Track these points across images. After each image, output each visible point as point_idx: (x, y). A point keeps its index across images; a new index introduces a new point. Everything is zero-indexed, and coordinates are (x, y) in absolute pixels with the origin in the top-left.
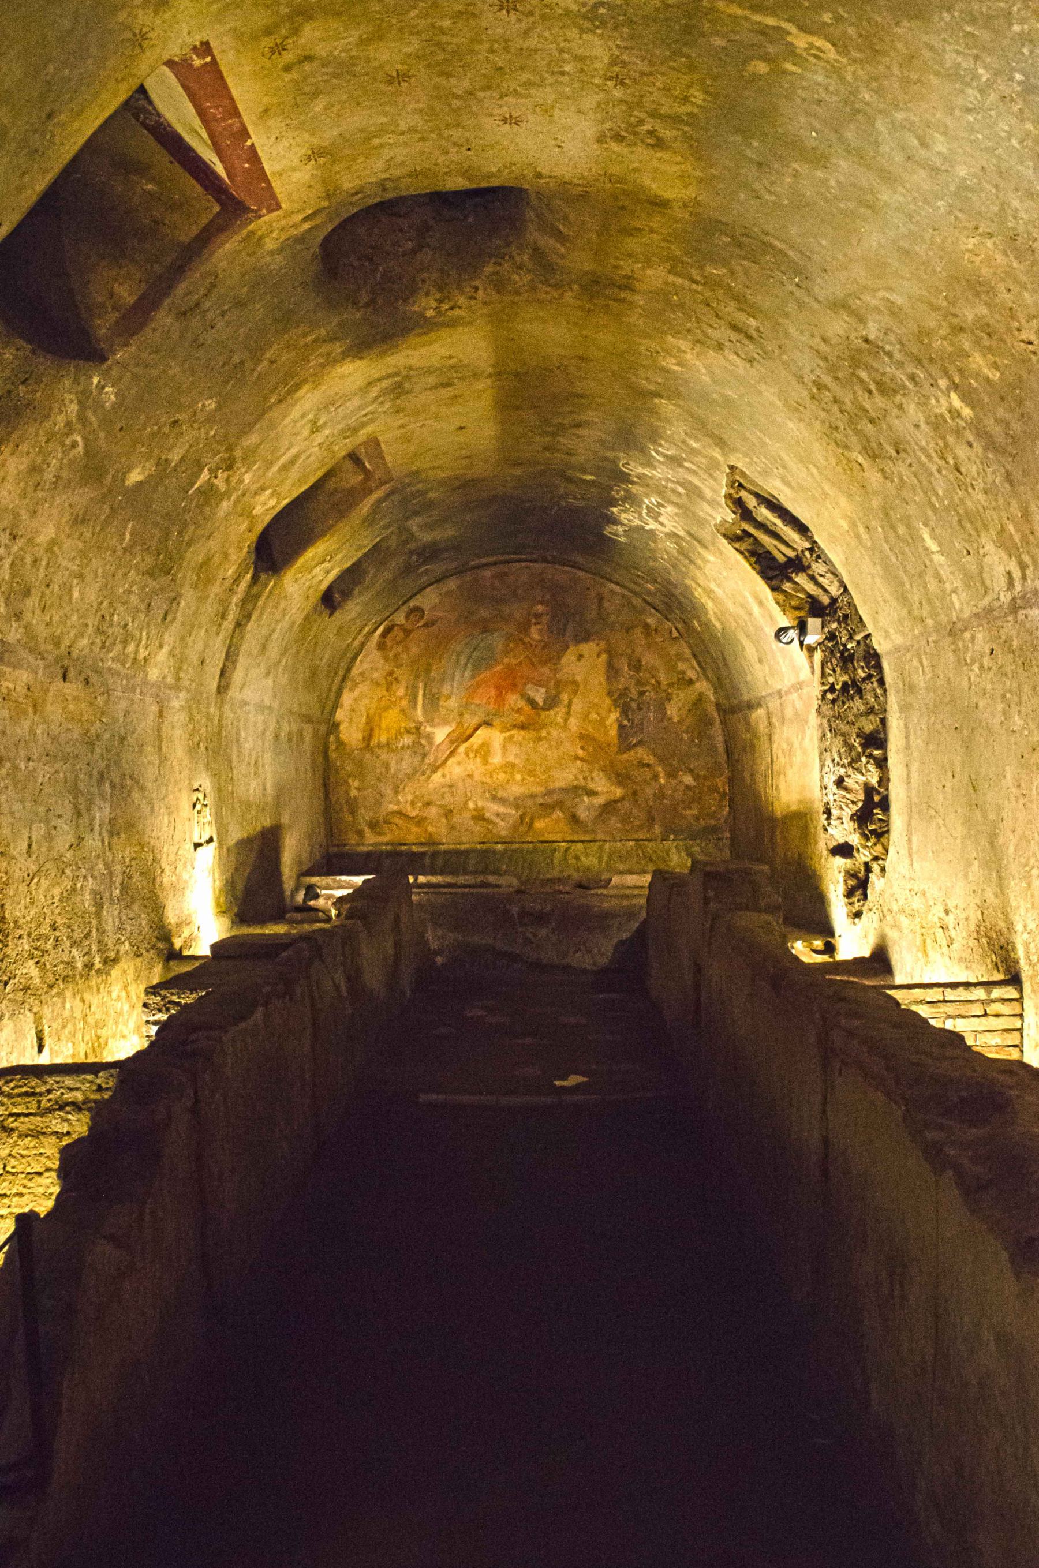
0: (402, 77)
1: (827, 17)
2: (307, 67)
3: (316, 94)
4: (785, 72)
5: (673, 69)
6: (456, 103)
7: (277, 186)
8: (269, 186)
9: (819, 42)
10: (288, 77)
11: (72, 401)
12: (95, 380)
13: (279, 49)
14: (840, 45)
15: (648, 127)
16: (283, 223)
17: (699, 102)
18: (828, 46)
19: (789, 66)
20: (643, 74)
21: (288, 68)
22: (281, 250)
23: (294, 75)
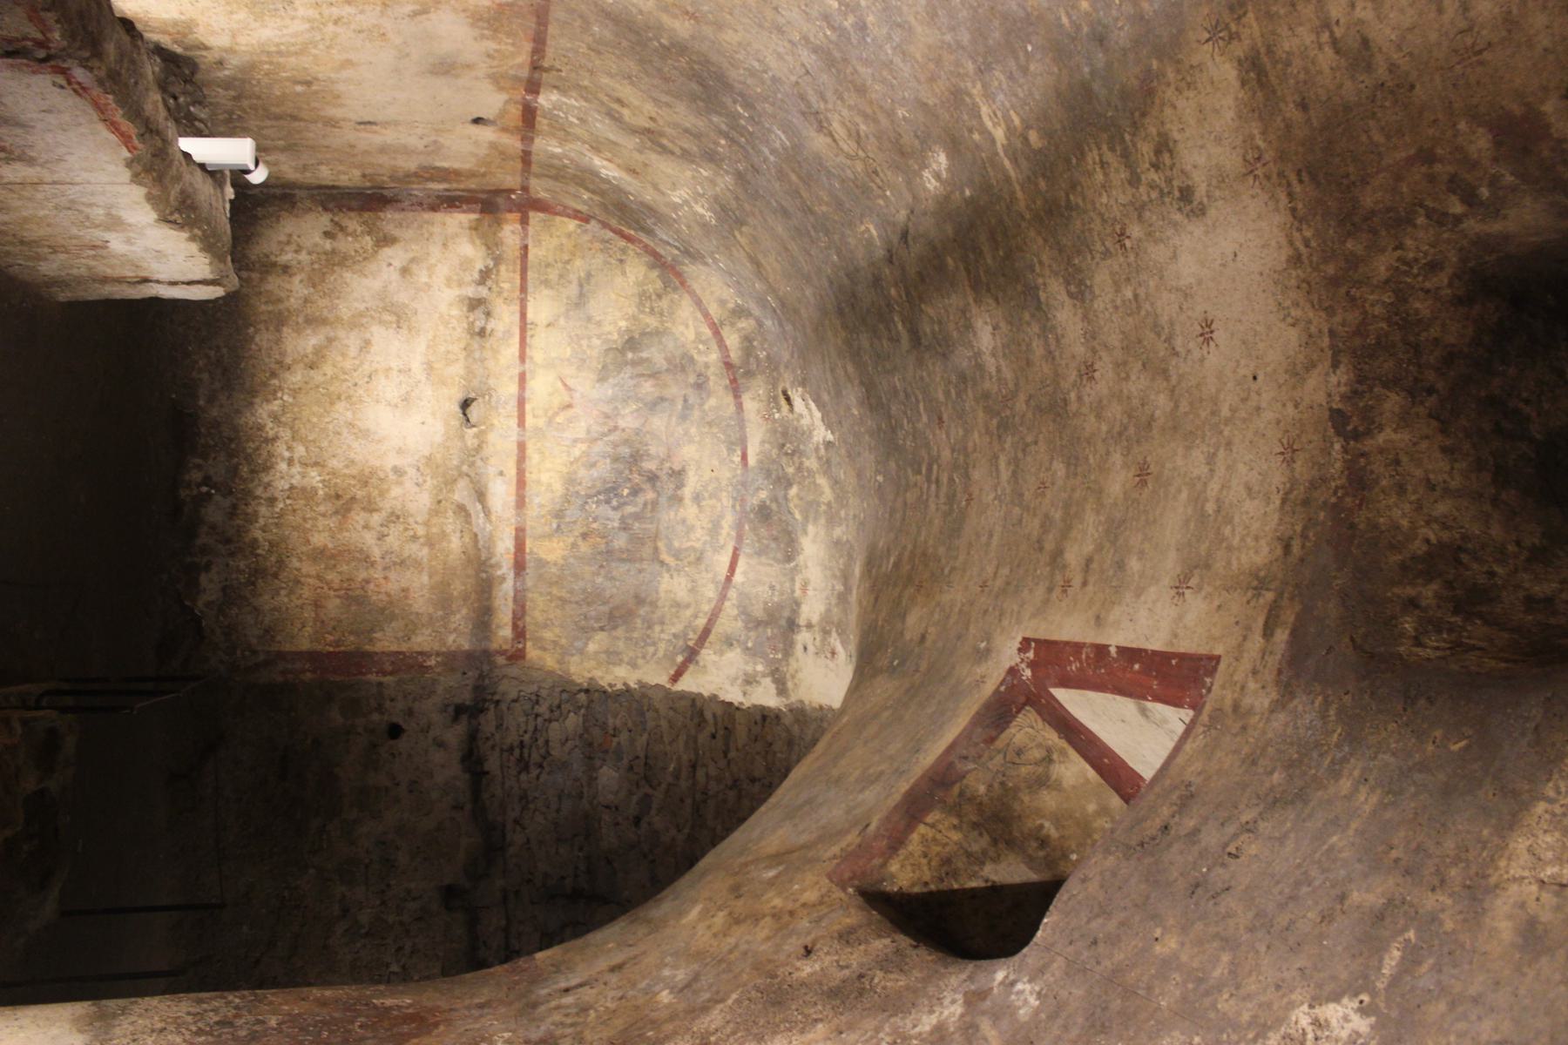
0: (1143, 474)
1: (976, 136)
2: (1094, 566)
3: (1120, 566)
4: (1022, 120)
5: (1084, 199)
6: (1184, 406)
7: (1184, 646)
8: (1182, 657)
9: (989, 124)
10: (1090, 588)
11: (953, 1002)
12: (1000, 976)
13: (1067, 585)
14: (975, 113)
15: (1153, 175)
16: (1246, 665)
17: (1095, 152)
18: (986, 120)
19: (1017, 121)
20: (1104, 221)
21: (1085, 584)
22: (1287, 691)
23: (1092, 580)
